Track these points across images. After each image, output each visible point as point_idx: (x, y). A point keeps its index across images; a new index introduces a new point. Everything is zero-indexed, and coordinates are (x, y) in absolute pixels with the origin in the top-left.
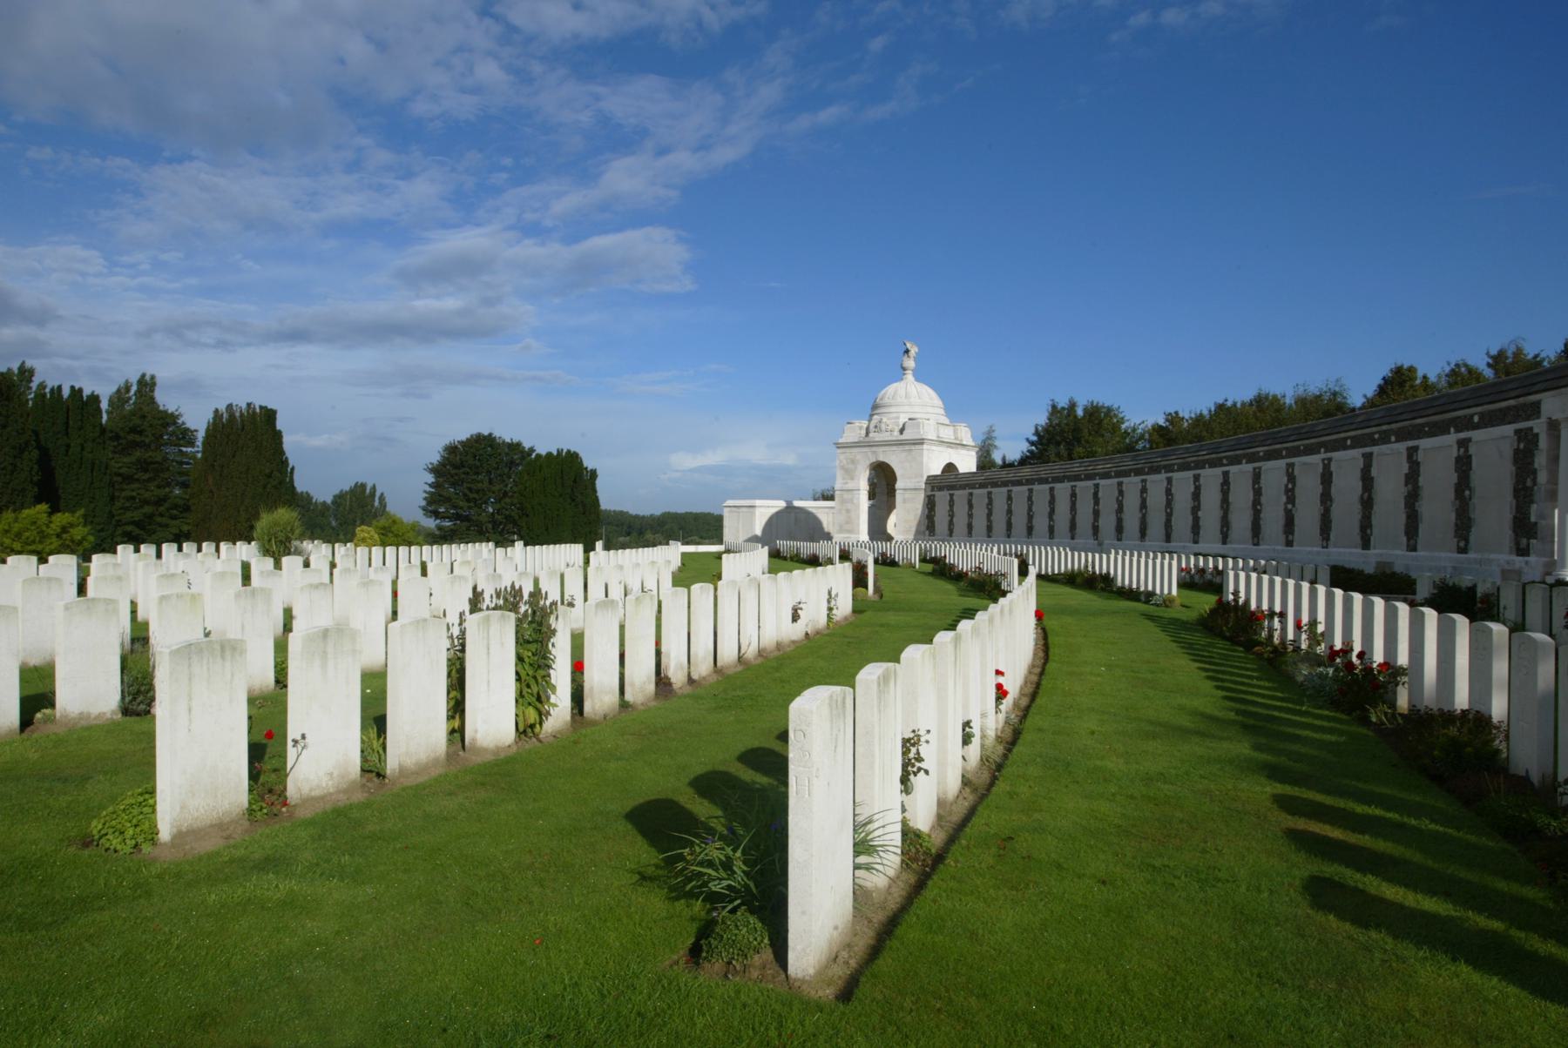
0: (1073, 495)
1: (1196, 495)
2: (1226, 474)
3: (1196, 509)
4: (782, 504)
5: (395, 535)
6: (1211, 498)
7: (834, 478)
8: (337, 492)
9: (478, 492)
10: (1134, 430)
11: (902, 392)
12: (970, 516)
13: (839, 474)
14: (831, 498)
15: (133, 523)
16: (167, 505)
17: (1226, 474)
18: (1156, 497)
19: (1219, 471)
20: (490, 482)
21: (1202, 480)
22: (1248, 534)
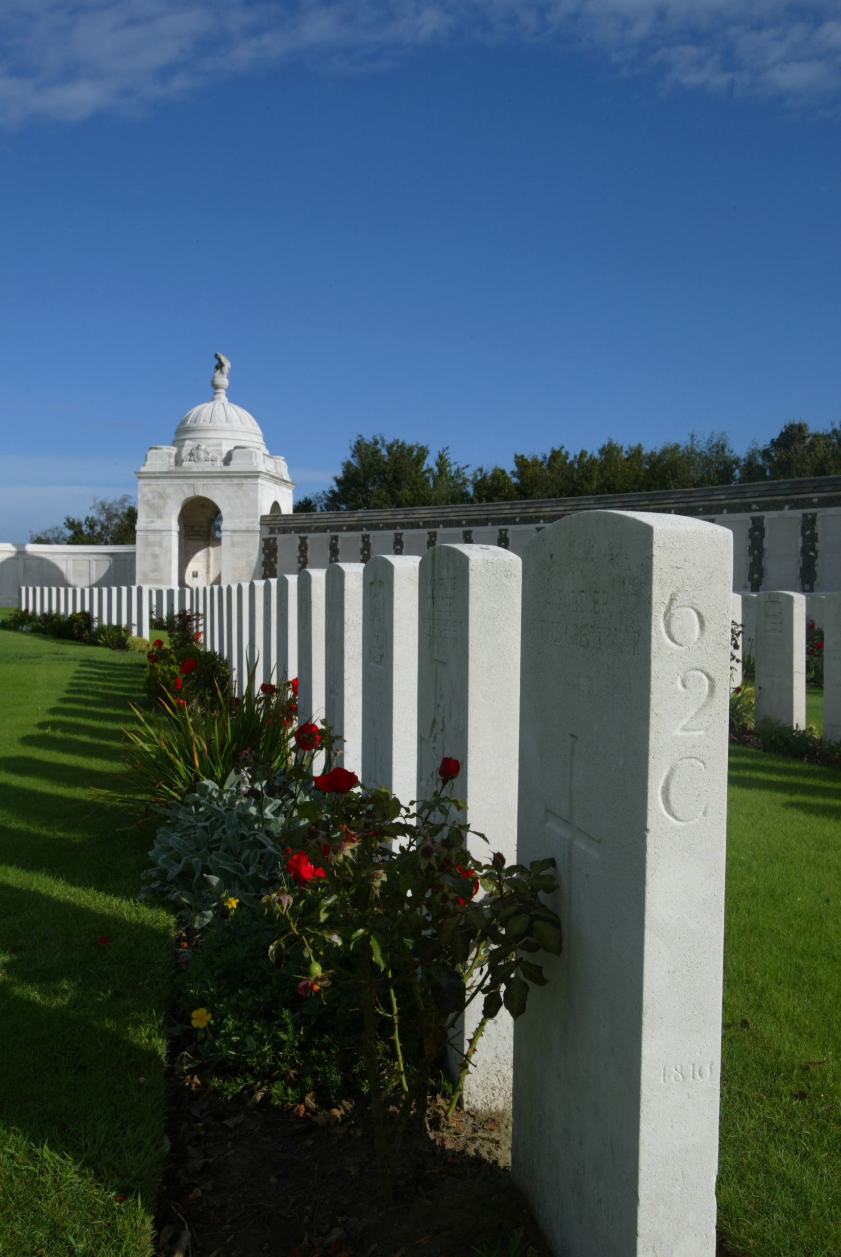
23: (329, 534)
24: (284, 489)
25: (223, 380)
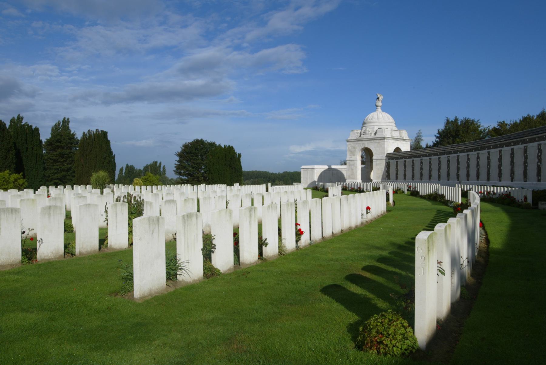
0: (449, 161)
1: (500, 160)
2: (513, 149)
3: (500, 166)
4: (326, 167)
5: (165, 182)
6: (506, 160)
7: (346, 156)
8: (145, 165)
9: (197, 164)
10: (485, 130)
11: (376, 116)
12: (405, 171)
13: (348, 154)
14: (345, 164)
15: (58, 179)
16: (71, 172)
17: (513, 149)
18: (483, 161)
19: (509, 148)
20: (202, 160)
21: (502, 153)
22: (522, 177)
23: (404, 160)
24: (404, 142)
25: (379, 103)
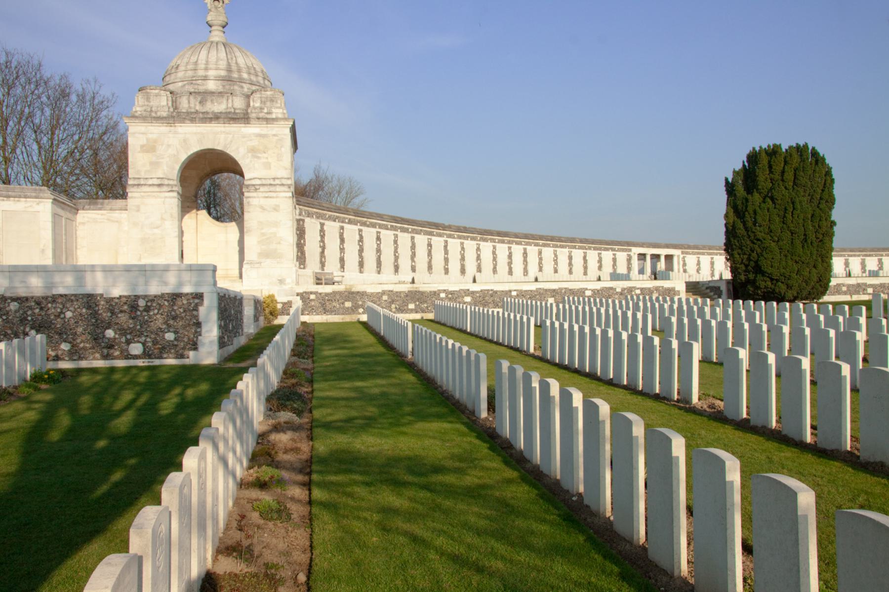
12: (342, 250)
